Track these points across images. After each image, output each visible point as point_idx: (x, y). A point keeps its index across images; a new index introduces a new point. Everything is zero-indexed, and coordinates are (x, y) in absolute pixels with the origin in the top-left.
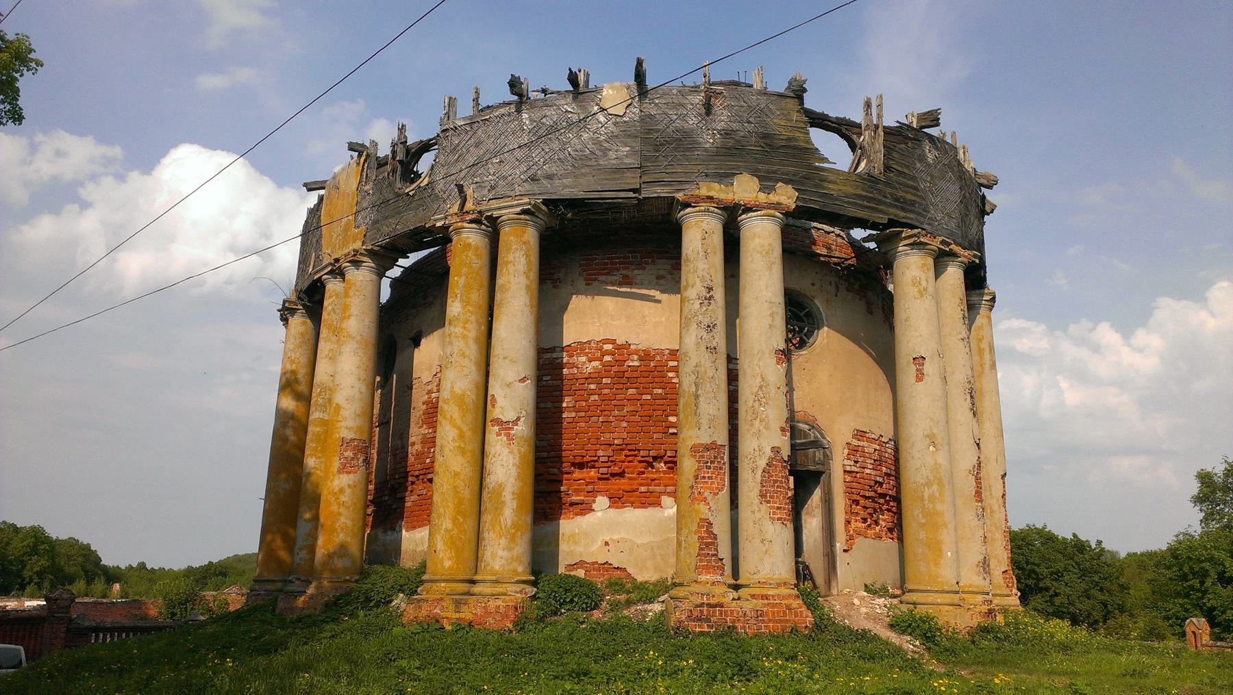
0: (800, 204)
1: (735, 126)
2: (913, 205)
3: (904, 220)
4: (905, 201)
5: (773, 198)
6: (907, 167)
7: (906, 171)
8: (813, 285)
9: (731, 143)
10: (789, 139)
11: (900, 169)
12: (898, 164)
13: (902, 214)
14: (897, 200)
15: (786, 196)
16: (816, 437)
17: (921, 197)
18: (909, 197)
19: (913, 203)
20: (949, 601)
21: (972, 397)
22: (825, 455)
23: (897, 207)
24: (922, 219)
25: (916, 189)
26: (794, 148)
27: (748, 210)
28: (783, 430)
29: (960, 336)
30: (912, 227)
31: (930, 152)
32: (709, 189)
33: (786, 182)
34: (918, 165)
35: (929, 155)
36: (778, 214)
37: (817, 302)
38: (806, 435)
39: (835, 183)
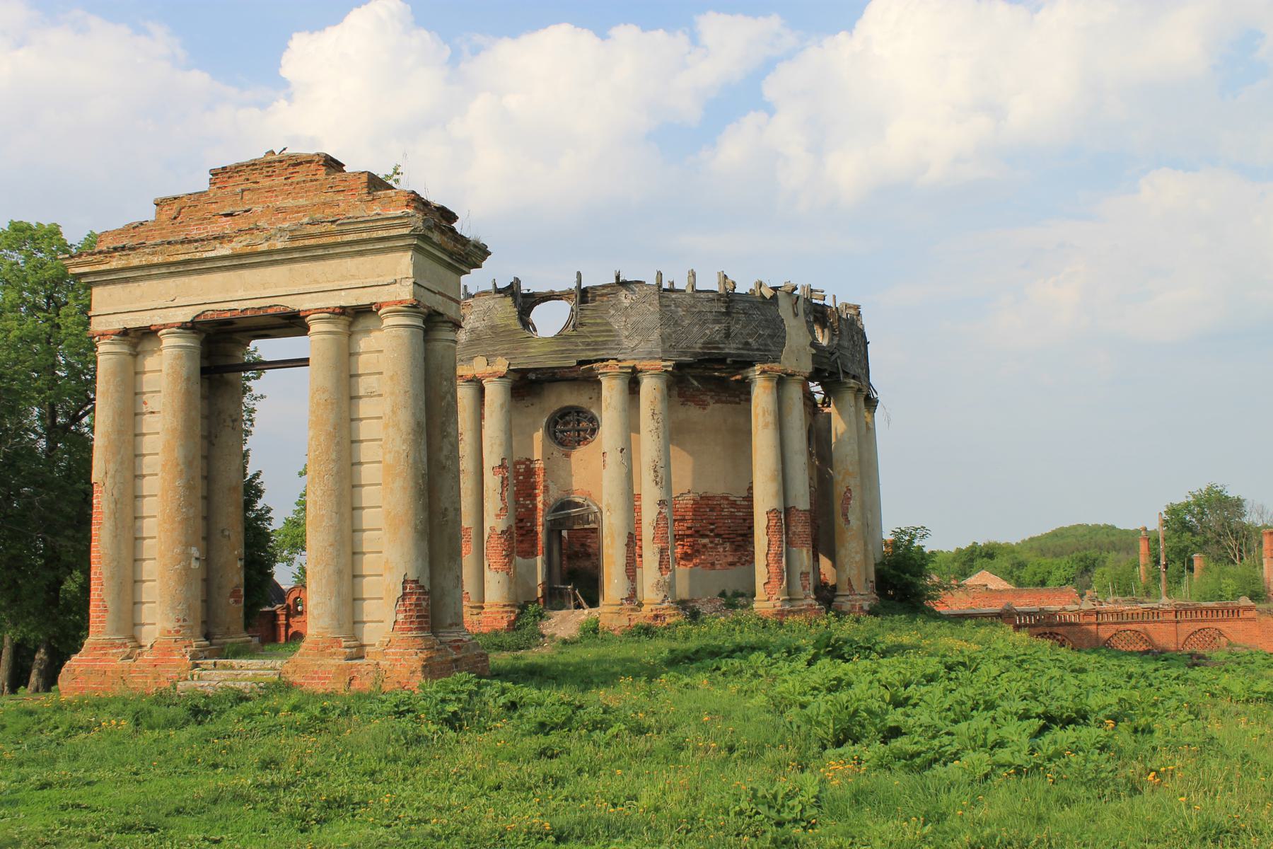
0: (511, 368)
1: (477, 324)
2: (605, 344)
3: (595, 358)
4: (596, 343)
5: (495, 368)
6: (600, 317)
7: (598, 321)
8: (591, 398)
9: (474, 336)
10: (506, 326)
11: (592, 321)
12: (591, 318)
13: (594, 353)
14: (588, 344)
15: (501, 366)
16: (588, 506)
17: (614, 336)
18: (600, 339)
19: (605, 343)
20: (609, 611)
21: (655, 471)
22: (596, 517)
23: (589, 350)
24: (614, 352)
25: (610, 331)
26: (509, 331)
27: (485, 377)
28: (497, 516)
29: (650, 429)
30: (603, 360)
31: (626, 298)
32: (463, 370)
33: (502, 355)
34: (613, 312)
35: (625, 301)
36: (494, 379)
37: (592, 410)
38: (582, 506)
39: (534, 347)
